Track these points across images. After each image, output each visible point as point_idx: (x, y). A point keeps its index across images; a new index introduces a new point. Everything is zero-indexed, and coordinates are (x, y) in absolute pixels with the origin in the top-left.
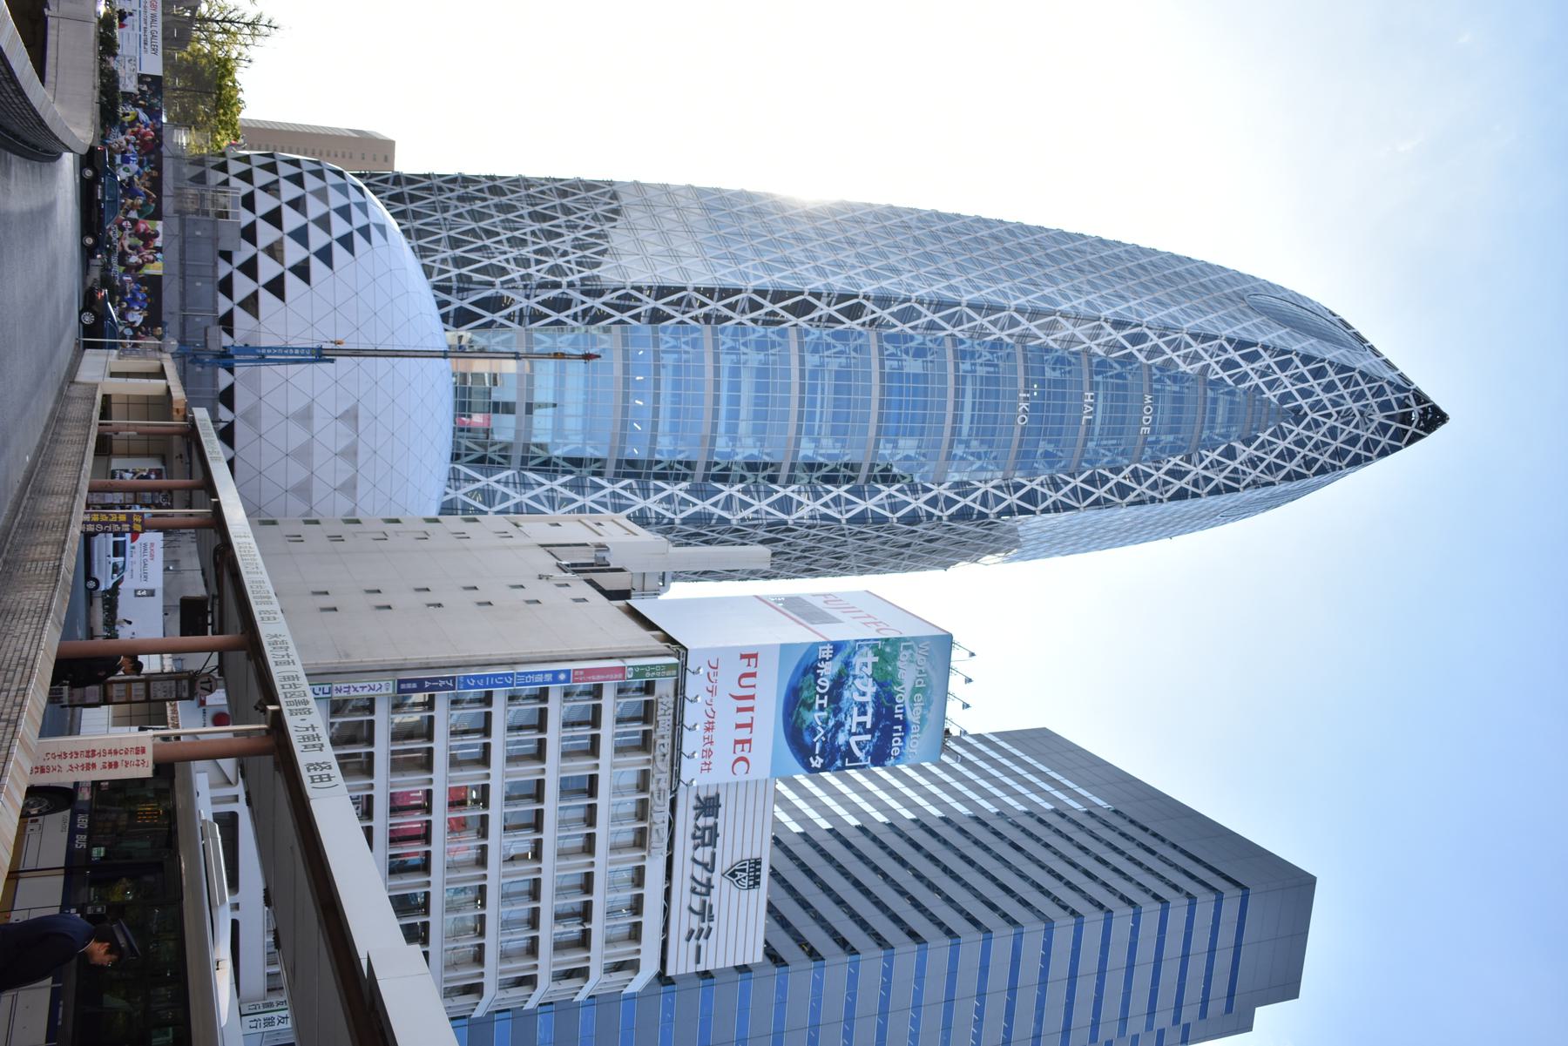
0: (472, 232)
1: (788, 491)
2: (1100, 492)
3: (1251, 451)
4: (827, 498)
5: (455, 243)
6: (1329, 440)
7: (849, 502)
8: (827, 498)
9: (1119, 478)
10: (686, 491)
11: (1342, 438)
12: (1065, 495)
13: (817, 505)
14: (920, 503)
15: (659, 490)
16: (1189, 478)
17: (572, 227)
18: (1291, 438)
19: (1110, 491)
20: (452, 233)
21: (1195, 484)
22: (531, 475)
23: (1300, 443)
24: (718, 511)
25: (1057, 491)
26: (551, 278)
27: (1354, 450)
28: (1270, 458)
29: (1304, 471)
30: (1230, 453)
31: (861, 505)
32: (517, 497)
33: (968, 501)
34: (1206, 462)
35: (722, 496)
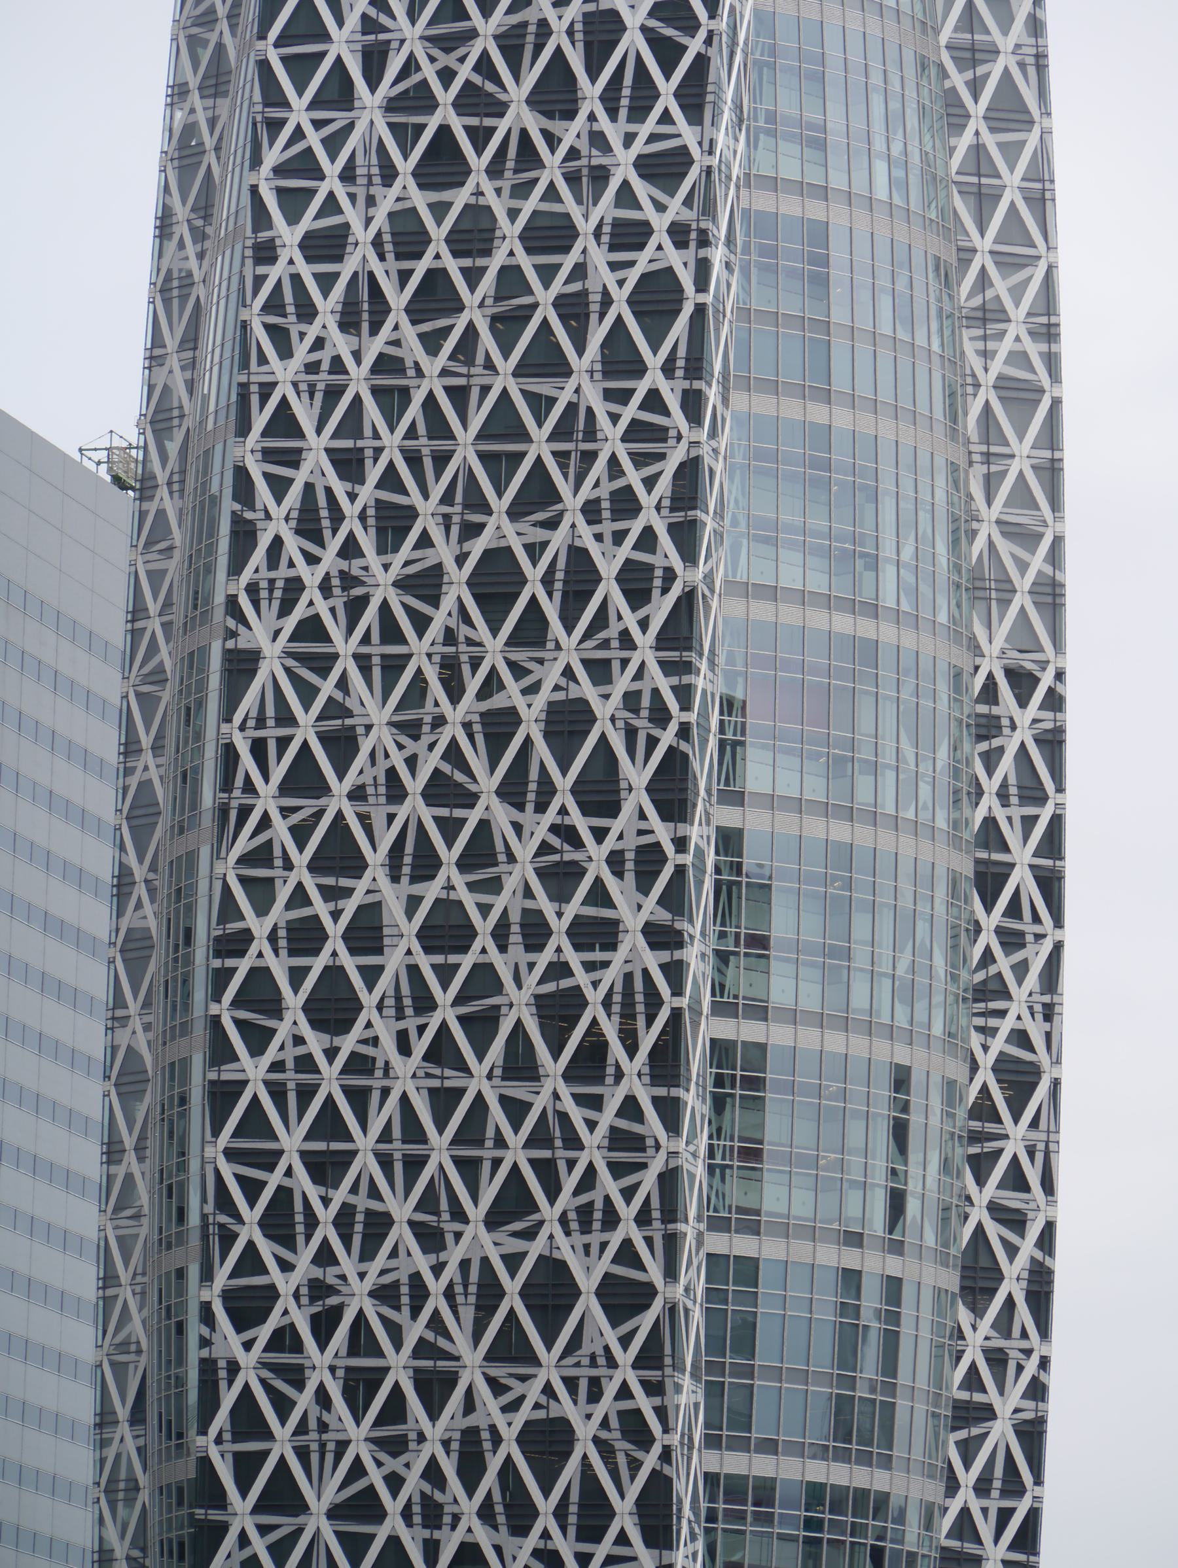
1: (986, 1061)
2: (1012, 180)
4: (1004, 964)
7: (1014, 909)
8: (1004, 964)
10: (978, 1311)
12: (1016, 293)
14: (1025, 717)
17: (432, 1514)
24: (1028, 1247)
31: (1021, 878)
33: (1024, 583)
35: (993, 1230)
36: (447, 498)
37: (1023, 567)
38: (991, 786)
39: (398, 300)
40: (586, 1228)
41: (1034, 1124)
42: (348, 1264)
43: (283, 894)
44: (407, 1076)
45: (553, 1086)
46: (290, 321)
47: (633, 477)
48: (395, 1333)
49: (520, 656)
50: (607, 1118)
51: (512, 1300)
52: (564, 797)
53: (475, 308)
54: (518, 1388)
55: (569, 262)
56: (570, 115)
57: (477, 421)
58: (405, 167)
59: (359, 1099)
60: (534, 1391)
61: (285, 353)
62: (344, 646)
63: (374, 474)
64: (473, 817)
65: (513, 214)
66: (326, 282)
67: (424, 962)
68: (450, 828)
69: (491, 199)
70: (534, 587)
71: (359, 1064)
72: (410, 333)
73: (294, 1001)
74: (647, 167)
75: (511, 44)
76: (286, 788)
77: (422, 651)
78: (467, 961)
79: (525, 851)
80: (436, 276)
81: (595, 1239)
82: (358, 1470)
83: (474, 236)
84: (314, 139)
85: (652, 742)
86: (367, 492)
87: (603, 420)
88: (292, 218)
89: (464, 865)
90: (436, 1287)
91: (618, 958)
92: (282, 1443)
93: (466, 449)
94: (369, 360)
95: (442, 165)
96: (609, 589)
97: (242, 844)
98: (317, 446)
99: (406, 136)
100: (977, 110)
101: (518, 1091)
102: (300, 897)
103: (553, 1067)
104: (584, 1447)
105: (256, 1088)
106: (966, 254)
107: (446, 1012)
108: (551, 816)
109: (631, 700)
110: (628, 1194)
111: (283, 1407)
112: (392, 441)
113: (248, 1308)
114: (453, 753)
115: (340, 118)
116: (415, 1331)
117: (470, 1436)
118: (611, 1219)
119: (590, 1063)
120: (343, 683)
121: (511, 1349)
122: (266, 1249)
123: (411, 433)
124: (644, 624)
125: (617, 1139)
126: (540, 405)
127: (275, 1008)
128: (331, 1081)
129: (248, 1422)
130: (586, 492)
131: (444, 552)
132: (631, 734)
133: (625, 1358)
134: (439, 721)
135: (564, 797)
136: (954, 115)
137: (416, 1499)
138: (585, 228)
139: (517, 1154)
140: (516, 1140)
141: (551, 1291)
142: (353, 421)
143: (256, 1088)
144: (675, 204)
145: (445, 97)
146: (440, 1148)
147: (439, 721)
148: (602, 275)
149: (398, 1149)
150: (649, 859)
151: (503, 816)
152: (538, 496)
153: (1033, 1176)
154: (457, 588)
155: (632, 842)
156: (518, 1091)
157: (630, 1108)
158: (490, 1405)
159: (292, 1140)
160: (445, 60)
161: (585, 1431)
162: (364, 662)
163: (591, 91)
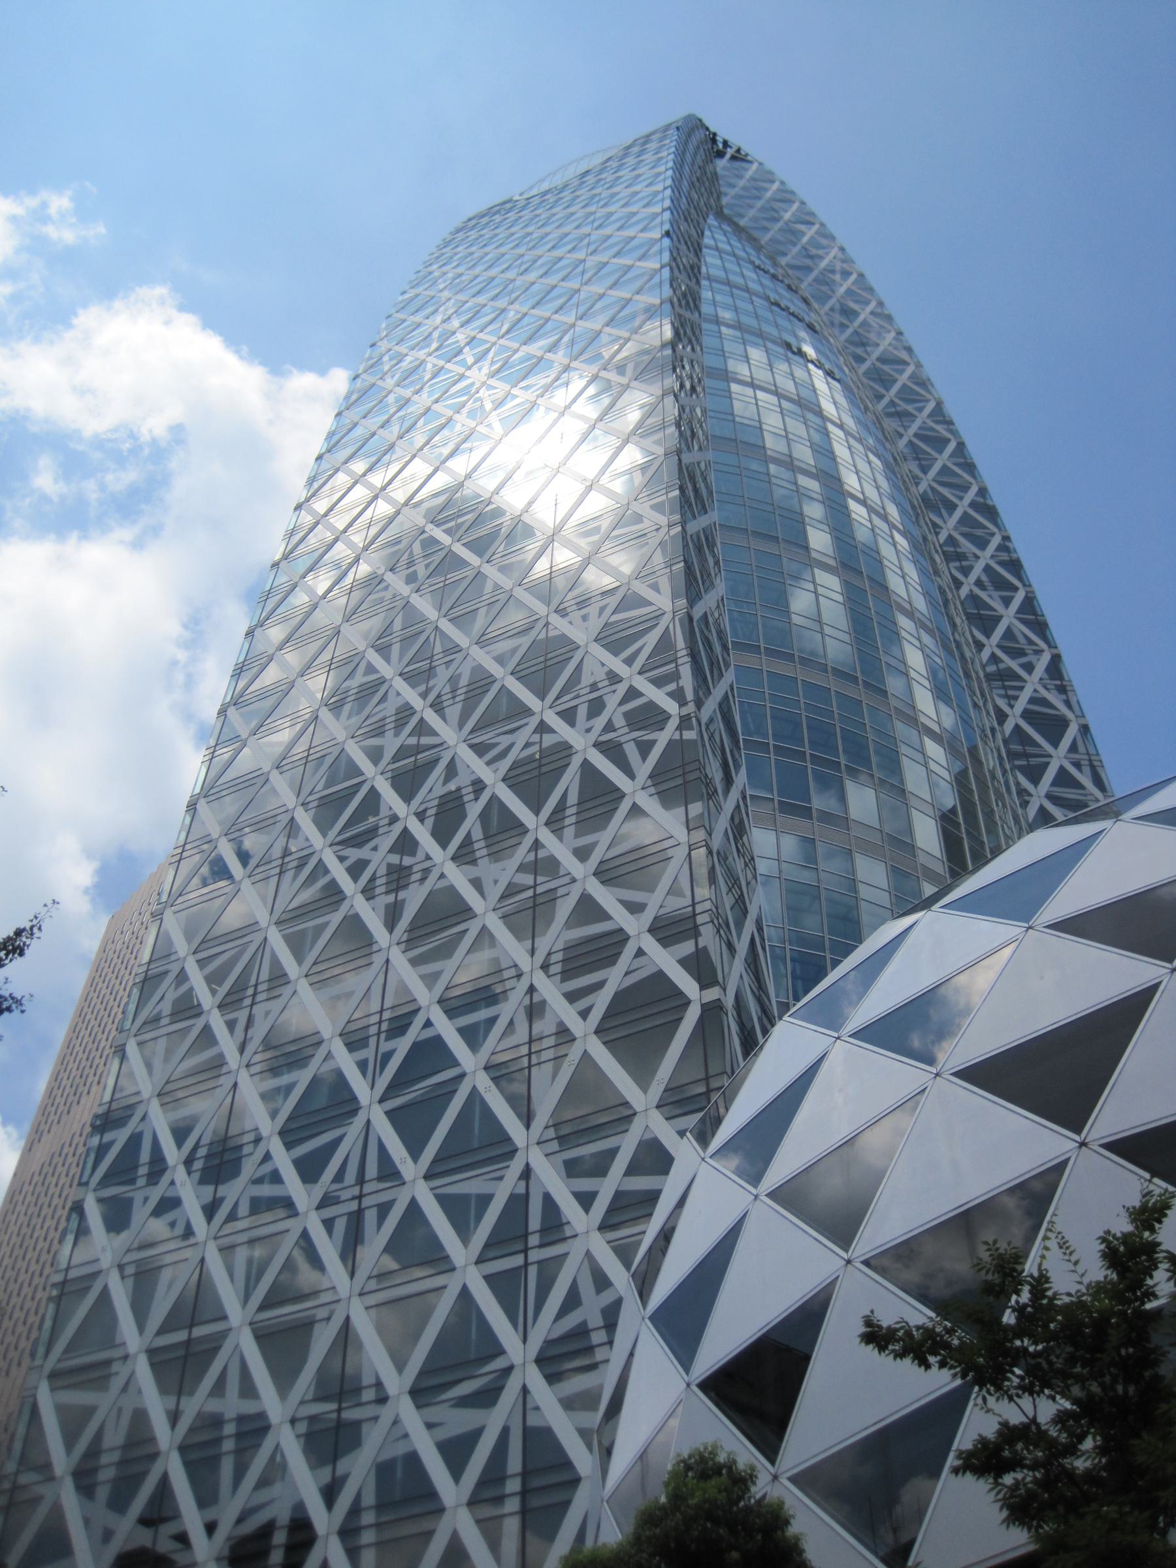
41: (1073, 748)
137: (383, 870)
153: (1085, 780)
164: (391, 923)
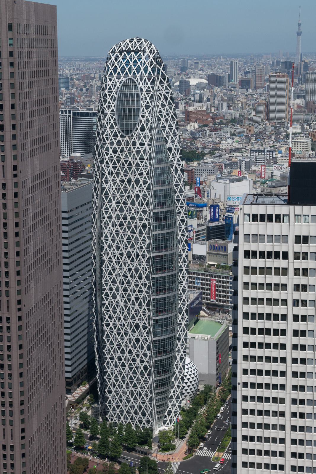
0: (131, 369)
1: (181, 289)
3: (169, 141)
4: (182, 279)
5: (134, 373)
6: (166, 108)
7: (183, 274)
8: (182, 279)
9: (178, 191)
11: (165, 103)
12: (182, 210)
13: (184, 282)
15: (180, 321)
16: (178, 167)
17: (126, 346)
18: (165, 124)
19: (181, 195)
20: (131, 373)
21: (179, 165)
22: (177, 349)
23: (167, 120)
24: (185, 307)
25: (181, 213)
26: (148, 357)
27: (169, 99)
28: (172, 134)
29: (175, 122)
30: (170, 149)
31: (184, 270)
32: (181, 352)
33: (184, 240)
34: (173, 159)
35: (182, 306)
36: (123, 246)
37: (183, 238)
38: (181, 262)
39: (118, 224)
40: (140, 320)
42: (117, 322)
43: (109, 285)
44: (122, 304)
45: (137, 306)
46: (106, 225)
47: (143, 245)
48: (122, 329)
49: (132, 262)
50: (142, 310)
51: (133, 327)
52: (137, 277)
53: (126, 225)
54: (134, 335)
55: (135, 221)
56: (135, 205)
57: (126, 238)
58: (118, 210)
59: (117, 306)
60: (136, 336)
61: (106, 229)
62: (114, 260)
63: (116, 242)
64: (128, 279)
65: (129, 216)
66: (110, 221)
67: (123, 293)
68: (125, 280)
69: (127, 214)
70: (133, 256)
71: (117, 302)
72: (119, 228)
73: (110, 296)
74: (142, 212)
75: (128, 197)
76: (108, 274)
77: (122, 261)
78: (128, 293)
79: (133, 283)
80: (121, 222)
81: (141, 321)
82: (119, 341)
83: (125, 218)
84: (108, 206)
85: (145, 273)
86: (115, 244)
87: (139, 239)
88: (106, 214)
89: (127, 283)
90: (126, 325)
91: (143, 294)
92: (111, 338)
93: (125, 241)
94: (115, 230)
95: (121, 210)
96: (140, 256)
97: (104, 279)
98: (110, 239)
99: (118, 206)
100: (178, 191)
101: (133, 306)
102: (110, 285)
103: (137, 304)
104: (141, 341)
105: (107, 304)
106: (177, 207)
107: (126, 298)
108: (135, 279)
109: (143, 268)
110: (145, 317)
111: (111, 335)
112: (118, 239)
113: (108, 325)
114: (125, 272)
115: (111, 204)
116: (124, 329)
117: (130, 339)
118: (143, 320)
119: (140, 305)
120: (114, 264)
121: (133, 331)
122: (109, 320)
123: (120, 238)
124: (144, 260)
125: (143, 312)
126: (133, 237)
127: (108, 296)
128: (114, 304)
129: (108, 336)
130: (138, 246)
131: (123, 251)
132: (143, 271)
133: (145, 333)
134: (124, 269)
135: (137, 277)
136: (176, 192)
138: (137, 218)
139: (133, 313)
140: (133, 311)
141: (137, 326)
142: (113, 237)
143: (107, 304)
144: (146, 216)
145: (122, 202)
146: (126, 311)
147: (124, 269)
148: (138, 223)
149: (121, 311)
150: (146, 285)
151: (130, 279)
152: (133, 246)
153: (186, 300)
154: (125, 255)
155: (144, 283)
156: (133, 306)
157: (144, 309)
158: (132, 336)
159: (111, 309)
160: (121, 198)
161: (141, 340)
162: (116, 262)
163: (137, 203)
164: (127, 351)
